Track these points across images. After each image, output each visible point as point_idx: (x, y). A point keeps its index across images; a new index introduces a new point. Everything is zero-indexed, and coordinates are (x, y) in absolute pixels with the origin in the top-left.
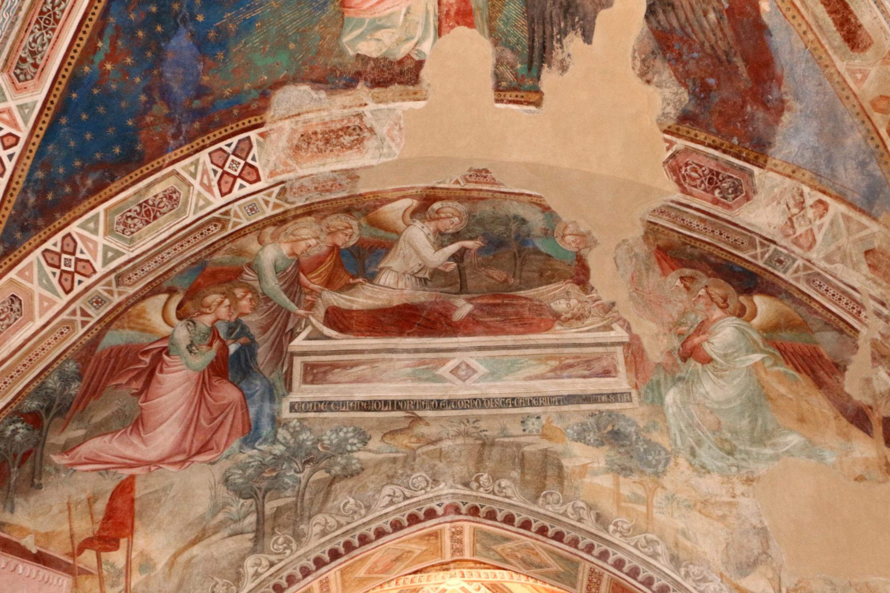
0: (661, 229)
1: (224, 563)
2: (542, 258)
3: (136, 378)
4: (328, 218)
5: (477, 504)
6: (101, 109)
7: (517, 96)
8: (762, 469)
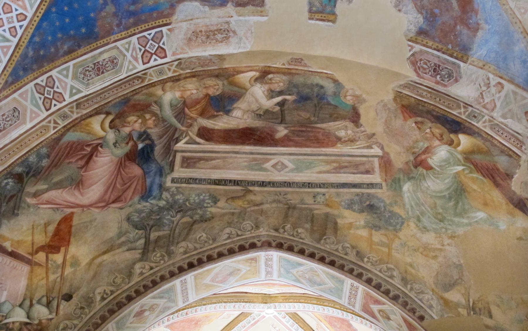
0: (404, 96)
1: (122, 266)
3: (81, 159)
4: (205, 80)
5: (282, 241)
7: (321, 16)
8: (460, 231)
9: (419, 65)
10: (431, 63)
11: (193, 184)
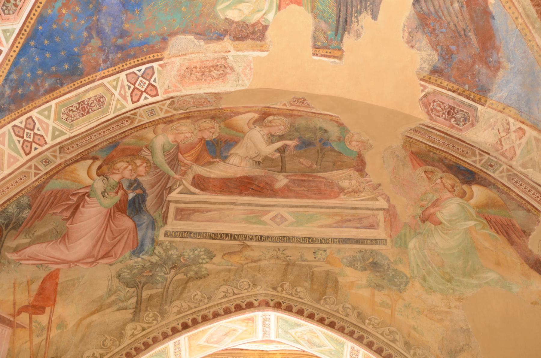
2: (336, 154)
3: (67, 209)
4: (200, 121)
5: (281, 301)
6: (57, 39)
7: (327, 52)
9: (431, 107)
10: (445, 105)
11: (188, 238)
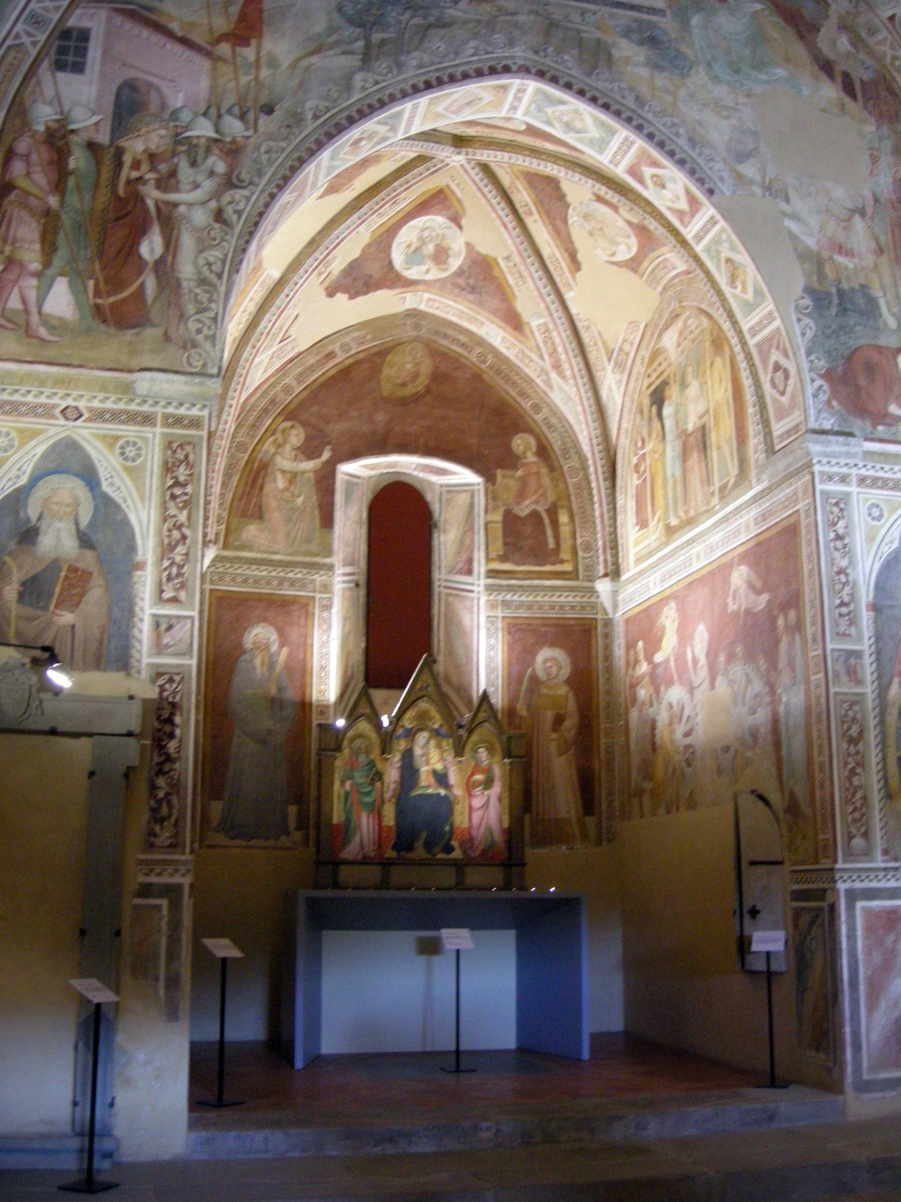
8: (758, 89)
